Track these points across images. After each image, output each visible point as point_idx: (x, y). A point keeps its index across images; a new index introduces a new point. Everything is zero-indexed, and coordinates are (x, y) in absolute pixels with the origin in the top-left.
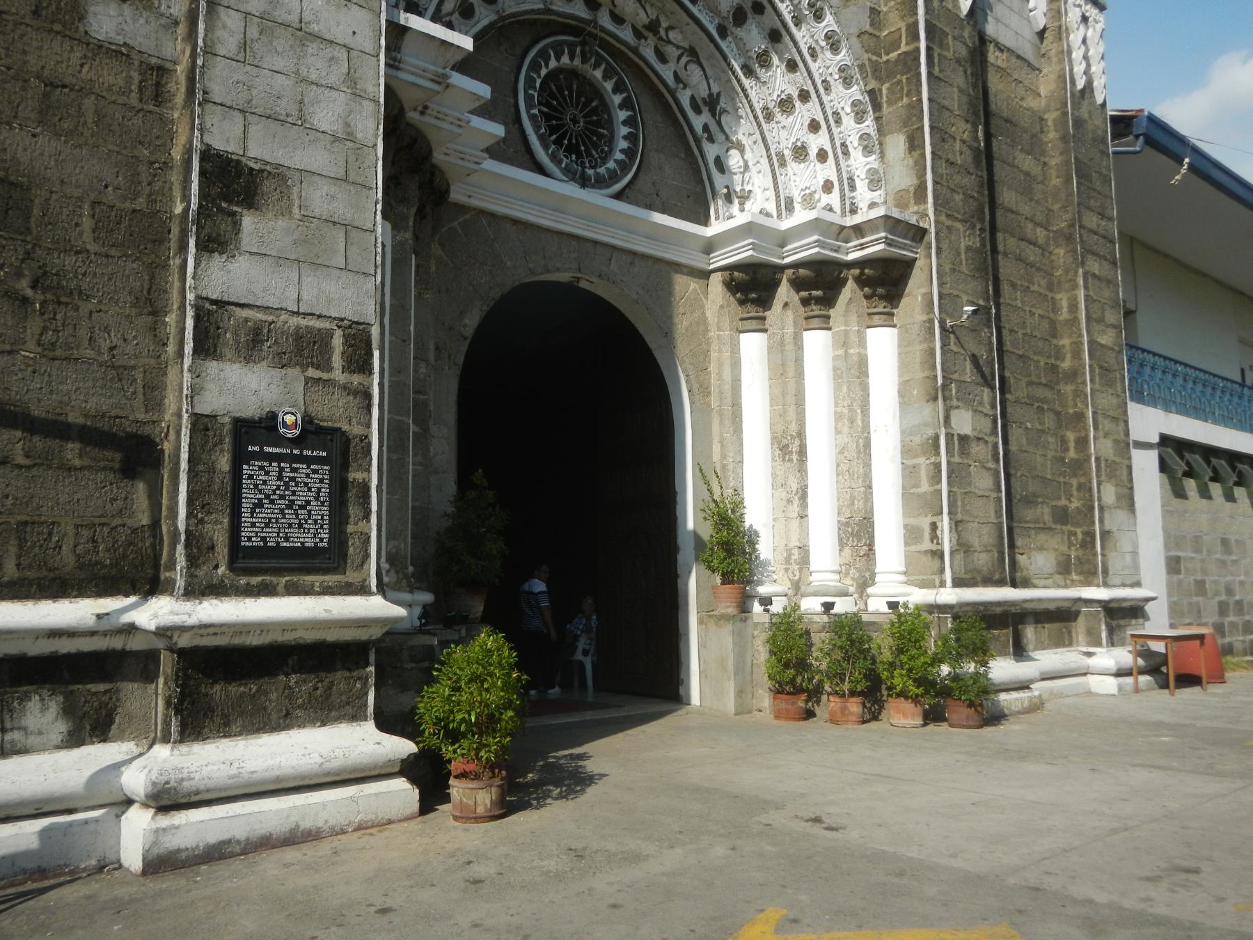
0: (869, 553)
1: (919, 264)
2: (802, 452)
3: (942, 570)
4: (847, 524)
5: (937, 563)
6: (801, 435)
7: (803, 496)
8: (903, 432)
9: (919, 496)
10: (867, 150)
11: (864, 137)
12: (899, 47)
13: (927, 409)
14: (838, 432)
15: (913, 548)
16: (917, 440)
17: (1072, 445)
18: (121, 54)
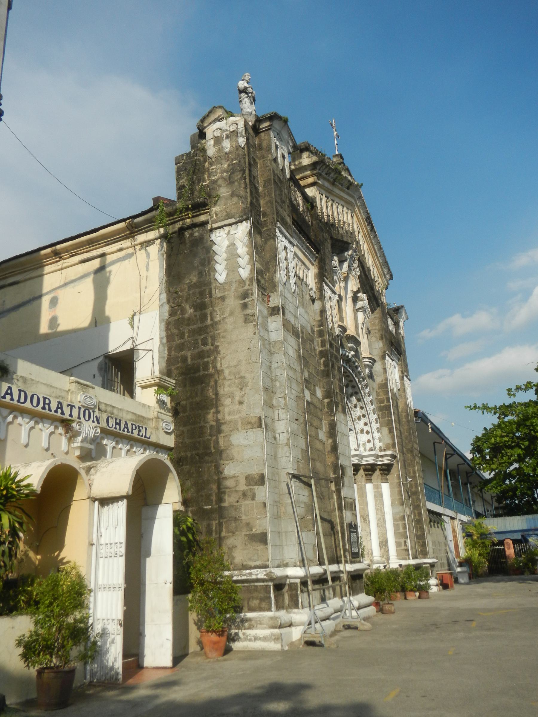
0: (388, 551)
1: (395, 465)
2: (369, 520)
3: (409, 555)
4: (382, 542)
5: (407, 553)
6: (368, 515)
7: (370, 533)
8: (393, 514)
9: (399, 533)
10: (378, 432)
11: (378, 428)
12: (384, 403)
13: (401, 508)
14: (377, 514)
15: (399, 548)
16: (398, 516)
17: (417, 514)
18: (321, 441)
